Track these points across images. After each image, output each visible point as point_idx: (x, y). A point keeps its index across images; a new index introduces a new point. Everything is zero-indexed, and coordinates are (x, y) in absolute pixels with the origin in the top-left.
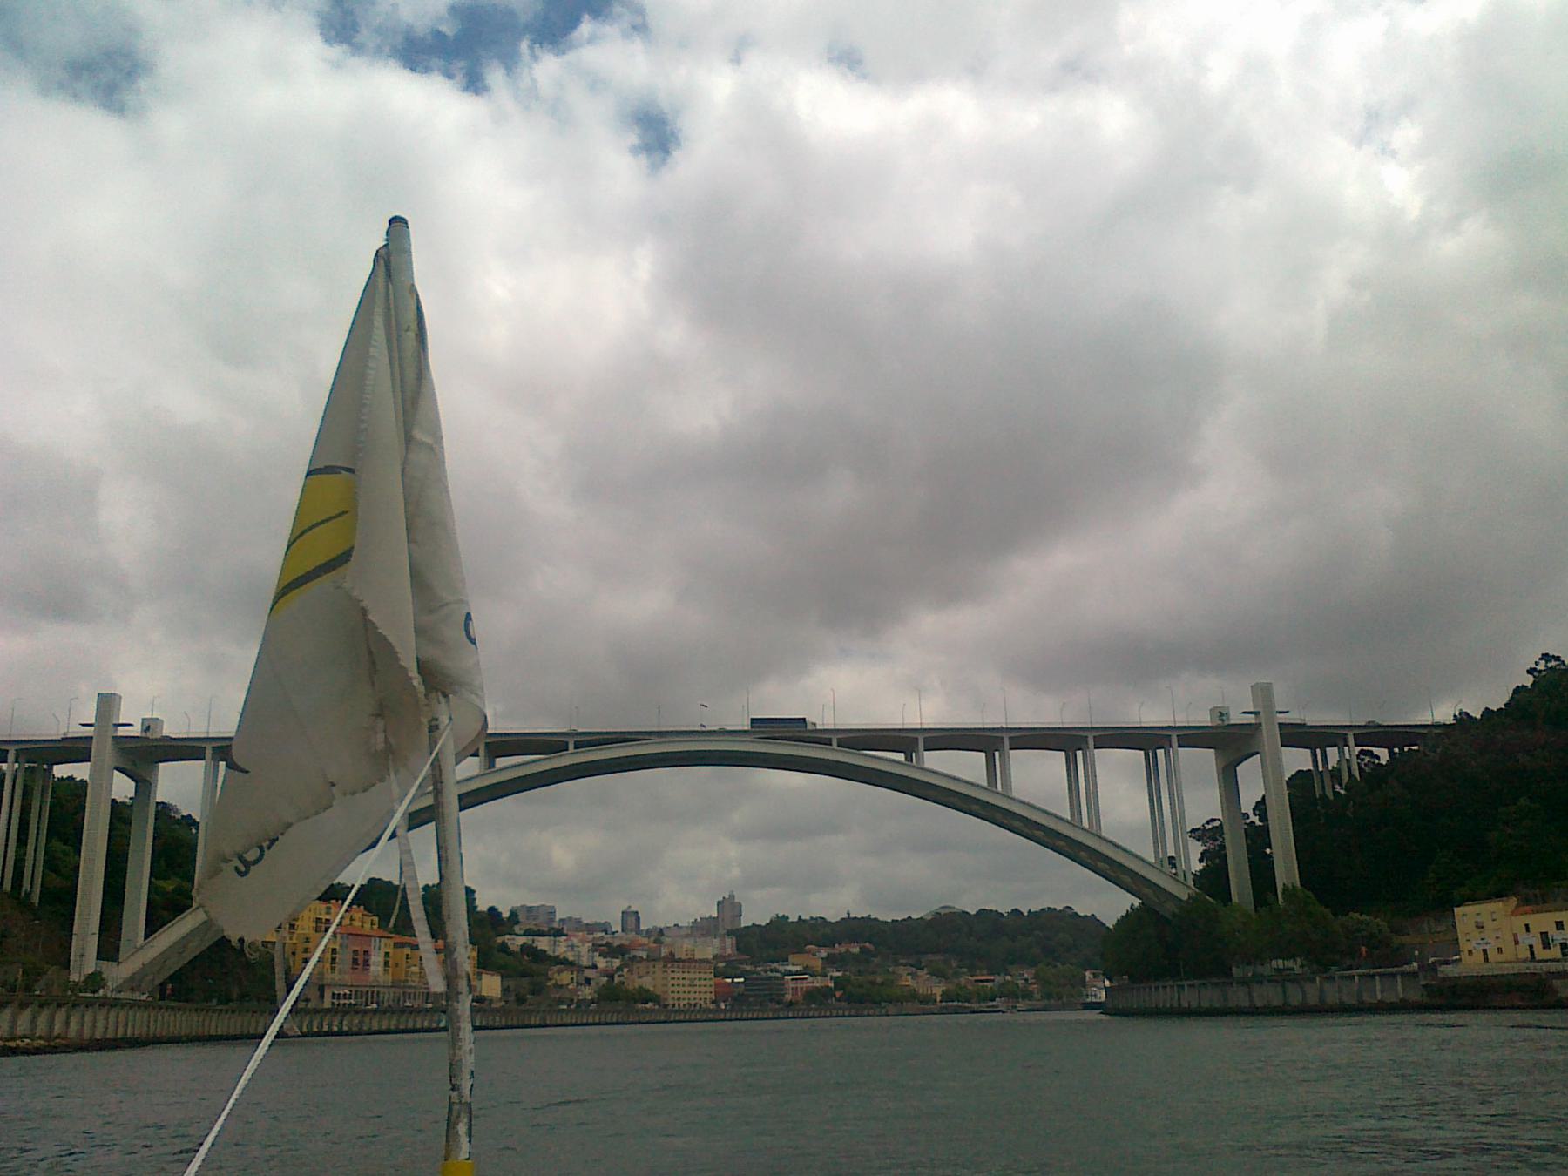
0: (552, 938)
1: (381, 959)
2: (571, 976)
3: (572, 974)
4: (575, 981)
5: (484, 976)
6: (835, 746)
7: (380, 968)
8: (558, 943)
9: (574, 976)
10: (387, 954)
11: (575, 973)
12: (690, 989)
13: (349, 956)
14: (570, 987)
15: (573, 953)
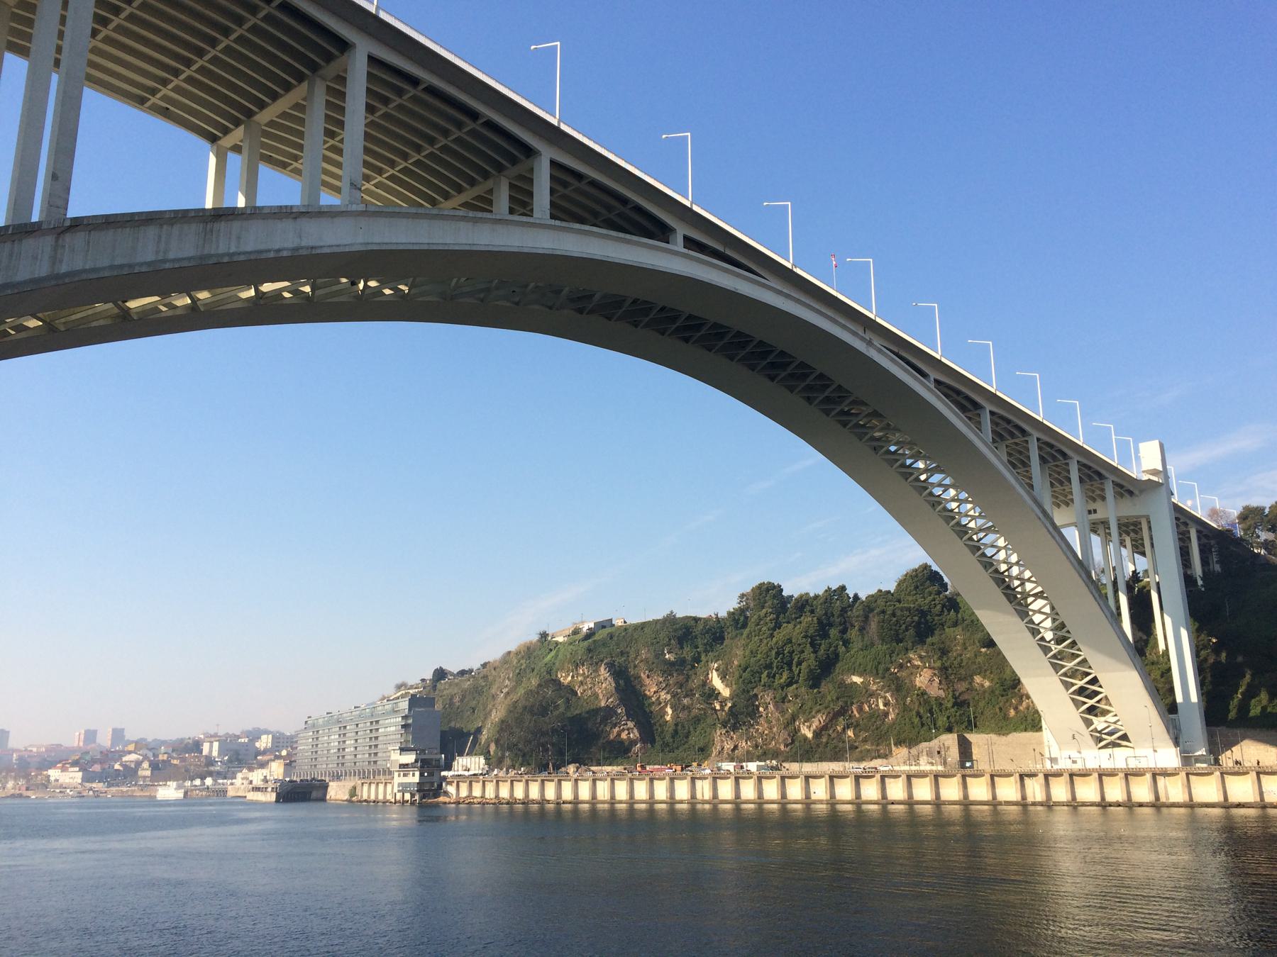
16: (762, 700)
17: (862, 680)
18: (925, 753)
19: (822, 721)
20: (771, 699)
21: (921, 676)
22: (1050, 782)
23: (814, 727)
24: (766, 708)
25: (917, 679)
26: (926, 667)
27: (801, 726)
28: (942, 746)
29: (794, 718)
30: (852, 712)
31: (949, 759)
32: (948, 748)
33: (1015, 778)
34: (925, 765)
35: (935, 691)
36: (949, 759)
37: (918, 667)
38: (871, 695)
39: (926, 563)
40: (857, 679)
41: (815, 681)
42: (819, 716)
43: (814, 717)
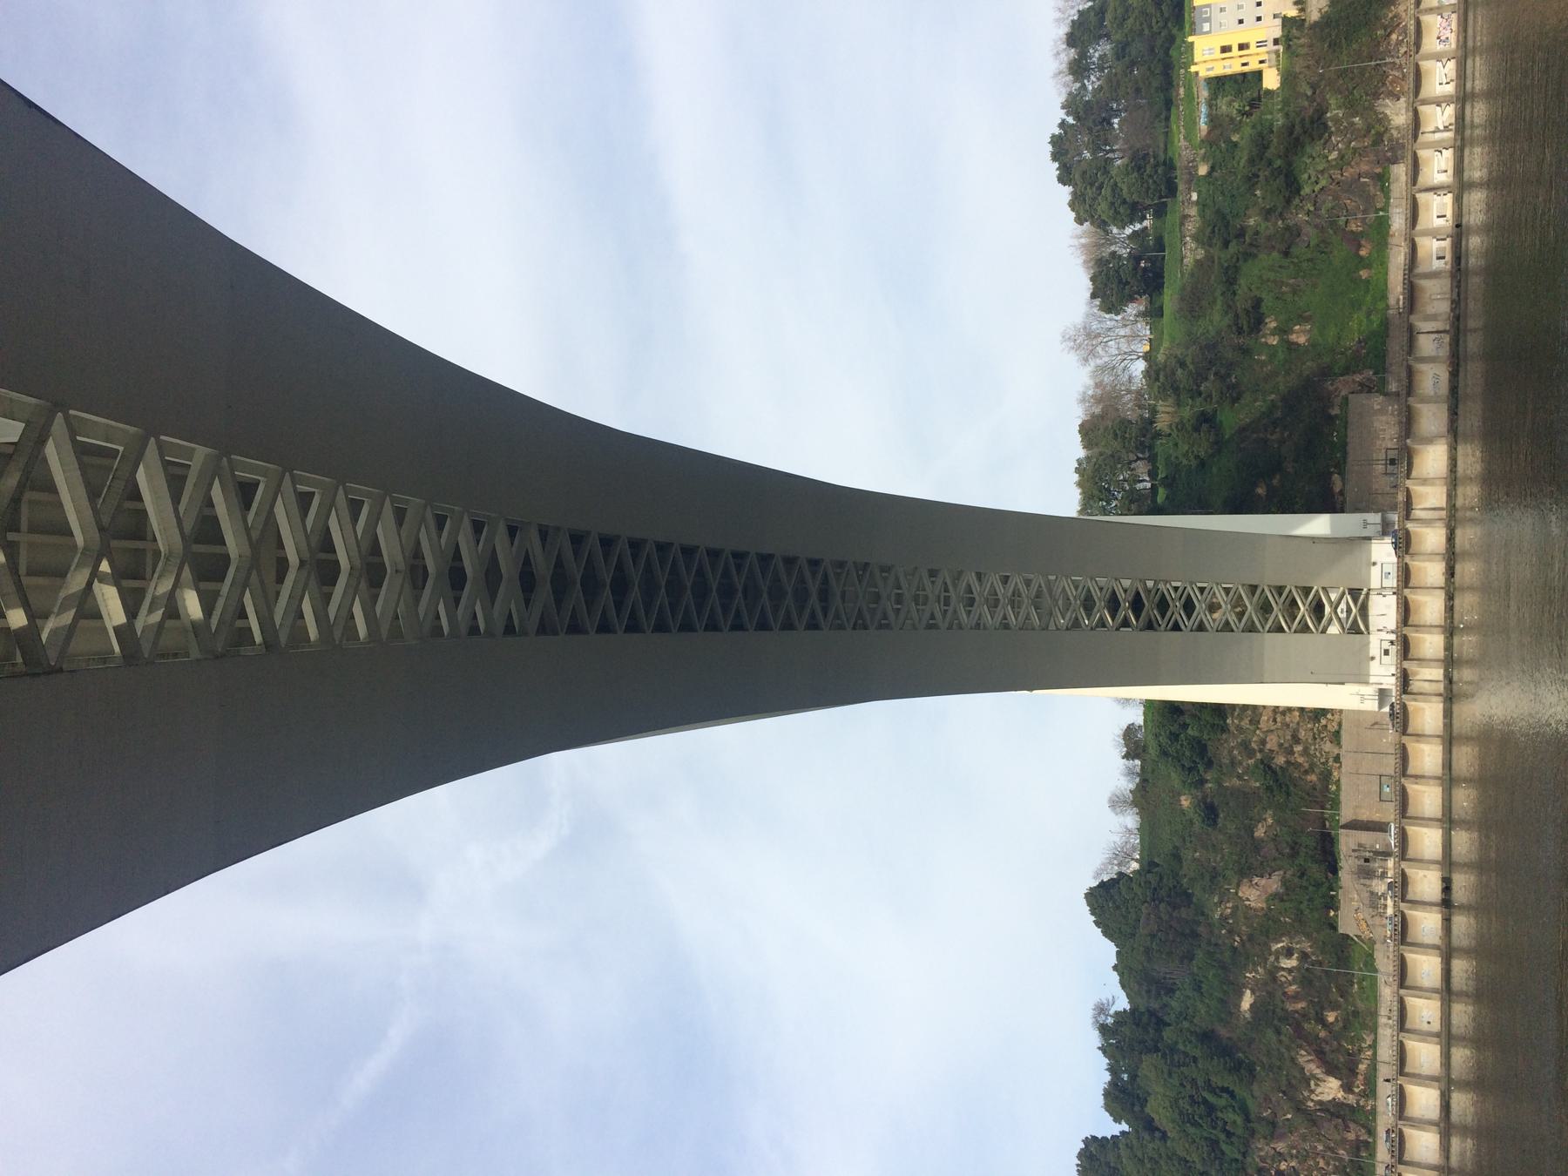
16: (1268, 1161)
17: (1248, 992)
18: (1367, 882)
19: (1310, 1058)
20: (1268, 1144)
21: (1248, 900)
22: (1415, 623)
23: (1317, 1071)
24: (1280, 1156)
25: (1253, 904)
26: (1237, 893)
27: (1316, 1098)
28: (1356, 854)
29: (1299, 1108)
30: (1296, 1012)
31: (1378, 847)
32: (1360, 845)
33: (1408, 700)
35: (1273, 884)
36: (1378, 847)
37: (1235, 908)
38: (1275, 979)
39: (1085, 894)
40: (1247, 1001)
41: (1244, 1069)
42: (1301, 1060)
43: (1303, 1069)
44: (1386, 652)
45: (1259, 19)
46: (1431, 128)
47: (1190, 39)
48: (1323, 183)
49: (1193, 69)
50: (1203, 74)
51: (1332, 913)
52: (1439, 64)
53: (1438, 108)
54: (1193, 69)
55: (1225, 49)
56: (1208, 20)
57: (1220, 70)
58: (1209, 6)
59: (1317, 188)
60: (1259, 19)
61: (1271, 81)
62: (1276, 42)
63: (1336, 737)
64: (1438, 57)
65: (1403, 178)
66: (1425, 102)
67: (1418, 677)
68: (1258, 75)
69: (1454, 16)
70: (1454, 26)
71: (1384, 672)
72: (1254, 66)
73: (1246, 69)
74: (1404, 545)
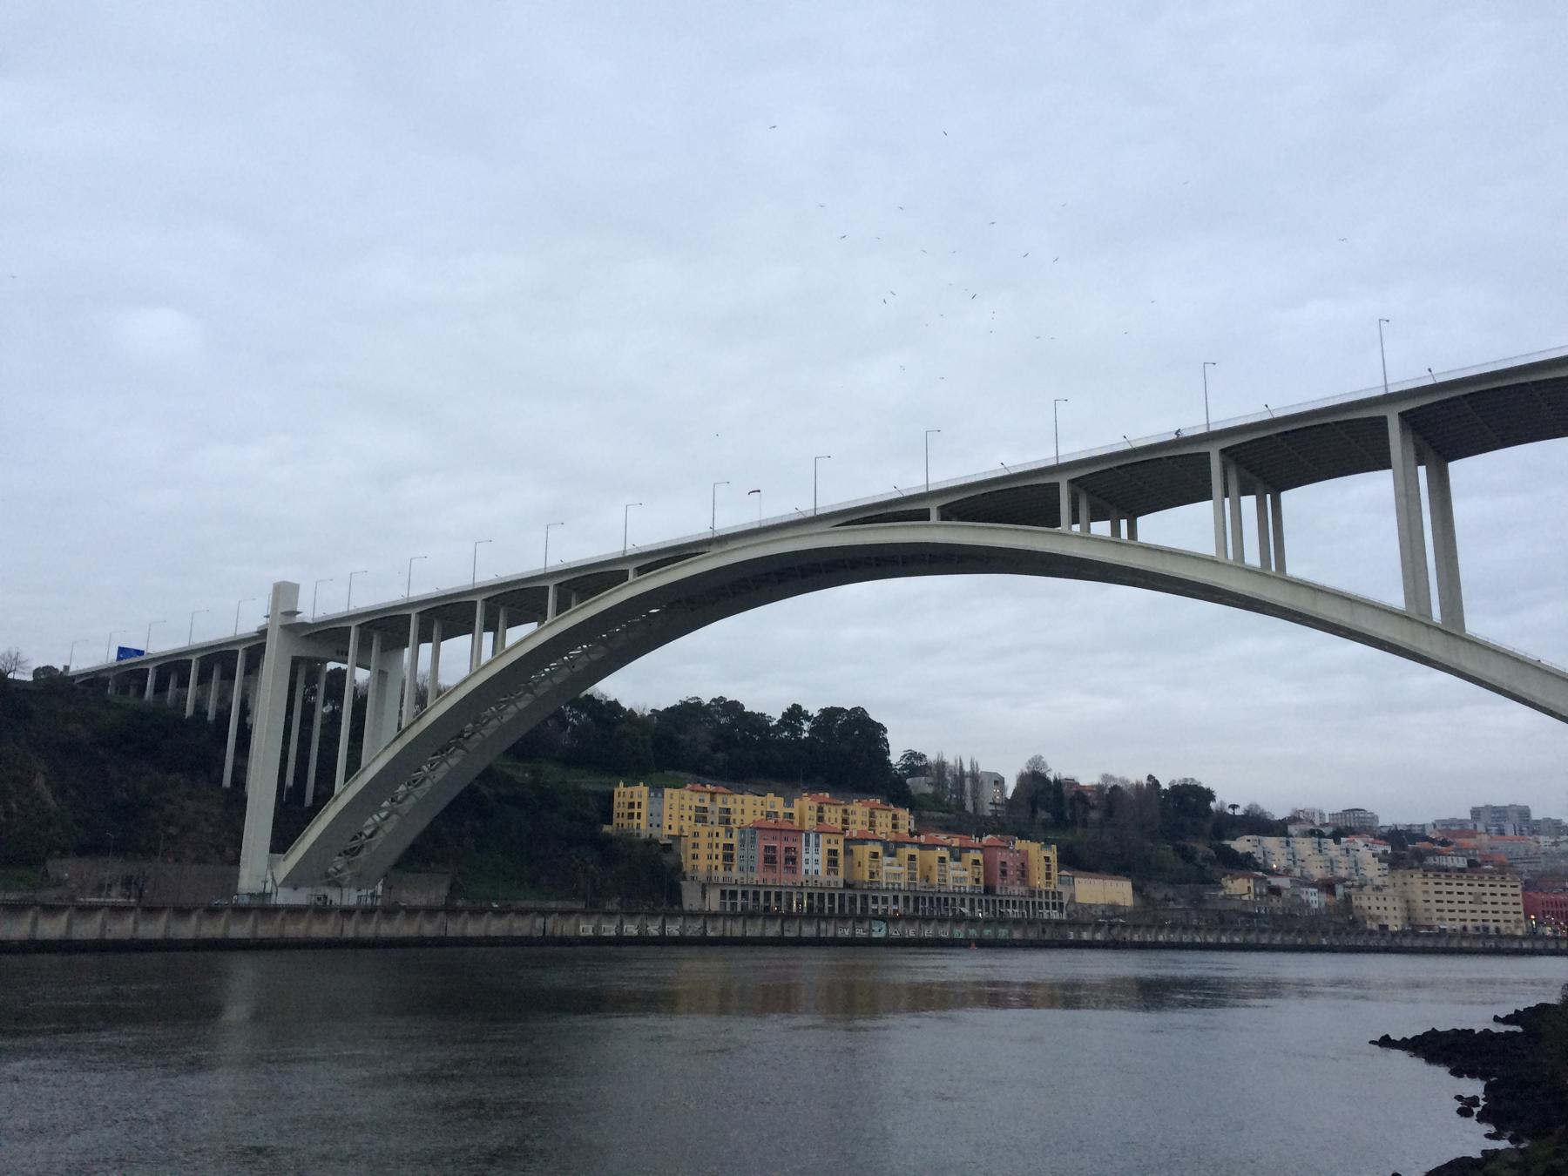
0: (1317, 839)
1: (822, 856)
2: (1246, 885)
3: (1249, 882)
4: (1252, 891)
5: (1076, 880)
6: (934, 515)
7: (822, 867)
8: (1324, 846)
9: (1251, 885)
10: (833, 852)
11: (1252, 881)
12: (1473, 907)
13: (758, 853)
14: (1245, 898)
15: (1321, 858)
34: (117, 898)
44: (319, 899)
45: (651, 825)
46: (648, 924)
47: (641, 784)
48: (577, 861)
49: (621, 784)
50: (616, 791)
51: (58, 853)
52: (678, 927)
53: (657, 927)
54: (621, 784)
55: (639, 804)
56: (656, 795)
57: (616, 800)
58: (663, 795)
59: (573, 857)
60: (651, 825)
61: (607, 828)
62: (638, 835)
63: (200, 860)
64: (683, 927)
65: (579, 907)
66: (664, 922)
67: (346, 921)
68: (610, 822)
69: (699, 934)
70: (693, 935)
71: (283, 897)
72: (616, 820)
73: (615, 815)
74: (431, 912)
